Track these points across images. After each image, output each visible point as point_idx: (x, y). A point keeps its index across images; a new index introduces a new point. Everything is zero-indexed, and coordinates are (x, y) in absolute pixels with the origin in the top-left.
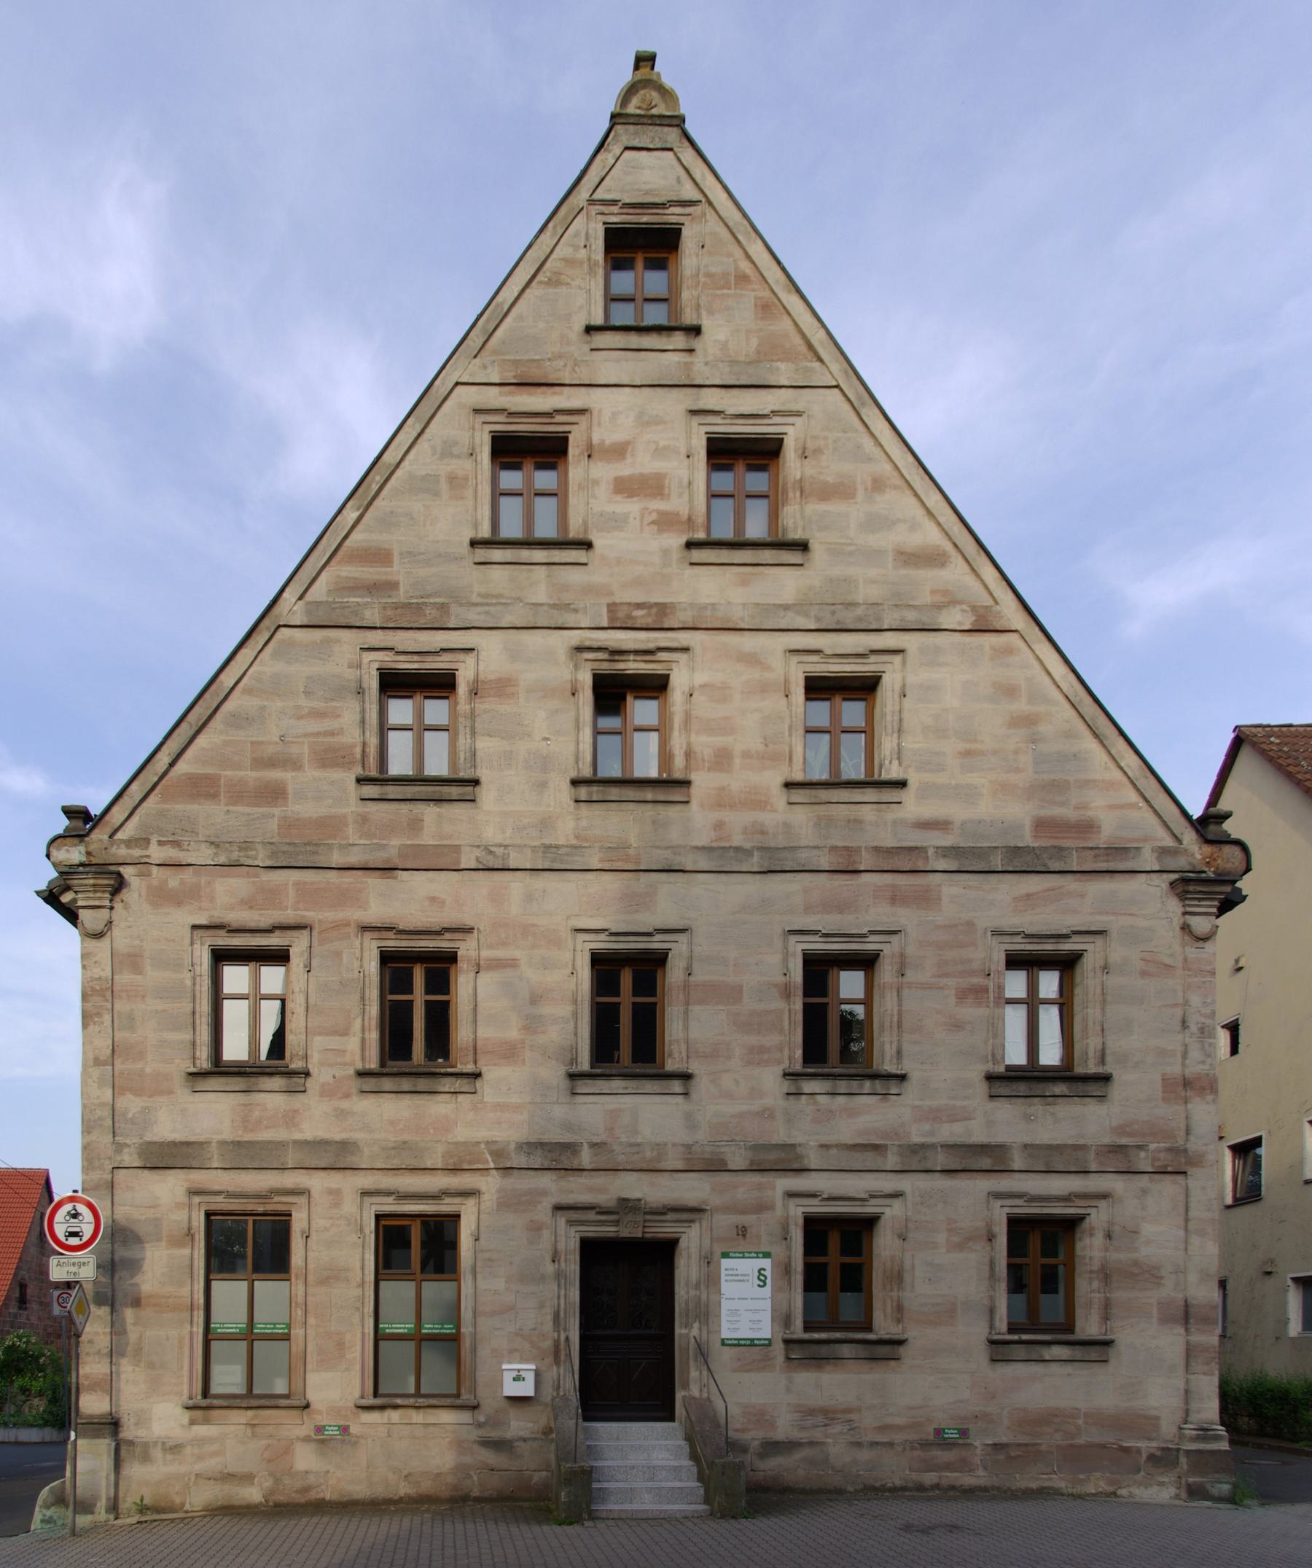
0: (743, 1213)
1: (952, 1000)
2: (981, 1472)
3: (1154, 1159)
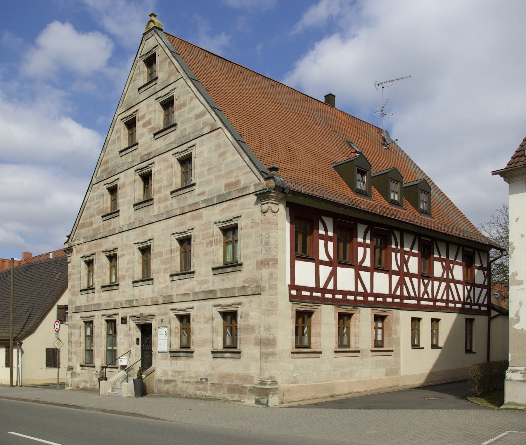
0: (162, 315)
1: (206, 246)
2: (209, 392)
3: (252, 290)
